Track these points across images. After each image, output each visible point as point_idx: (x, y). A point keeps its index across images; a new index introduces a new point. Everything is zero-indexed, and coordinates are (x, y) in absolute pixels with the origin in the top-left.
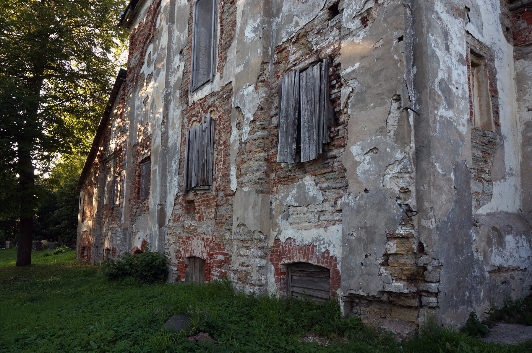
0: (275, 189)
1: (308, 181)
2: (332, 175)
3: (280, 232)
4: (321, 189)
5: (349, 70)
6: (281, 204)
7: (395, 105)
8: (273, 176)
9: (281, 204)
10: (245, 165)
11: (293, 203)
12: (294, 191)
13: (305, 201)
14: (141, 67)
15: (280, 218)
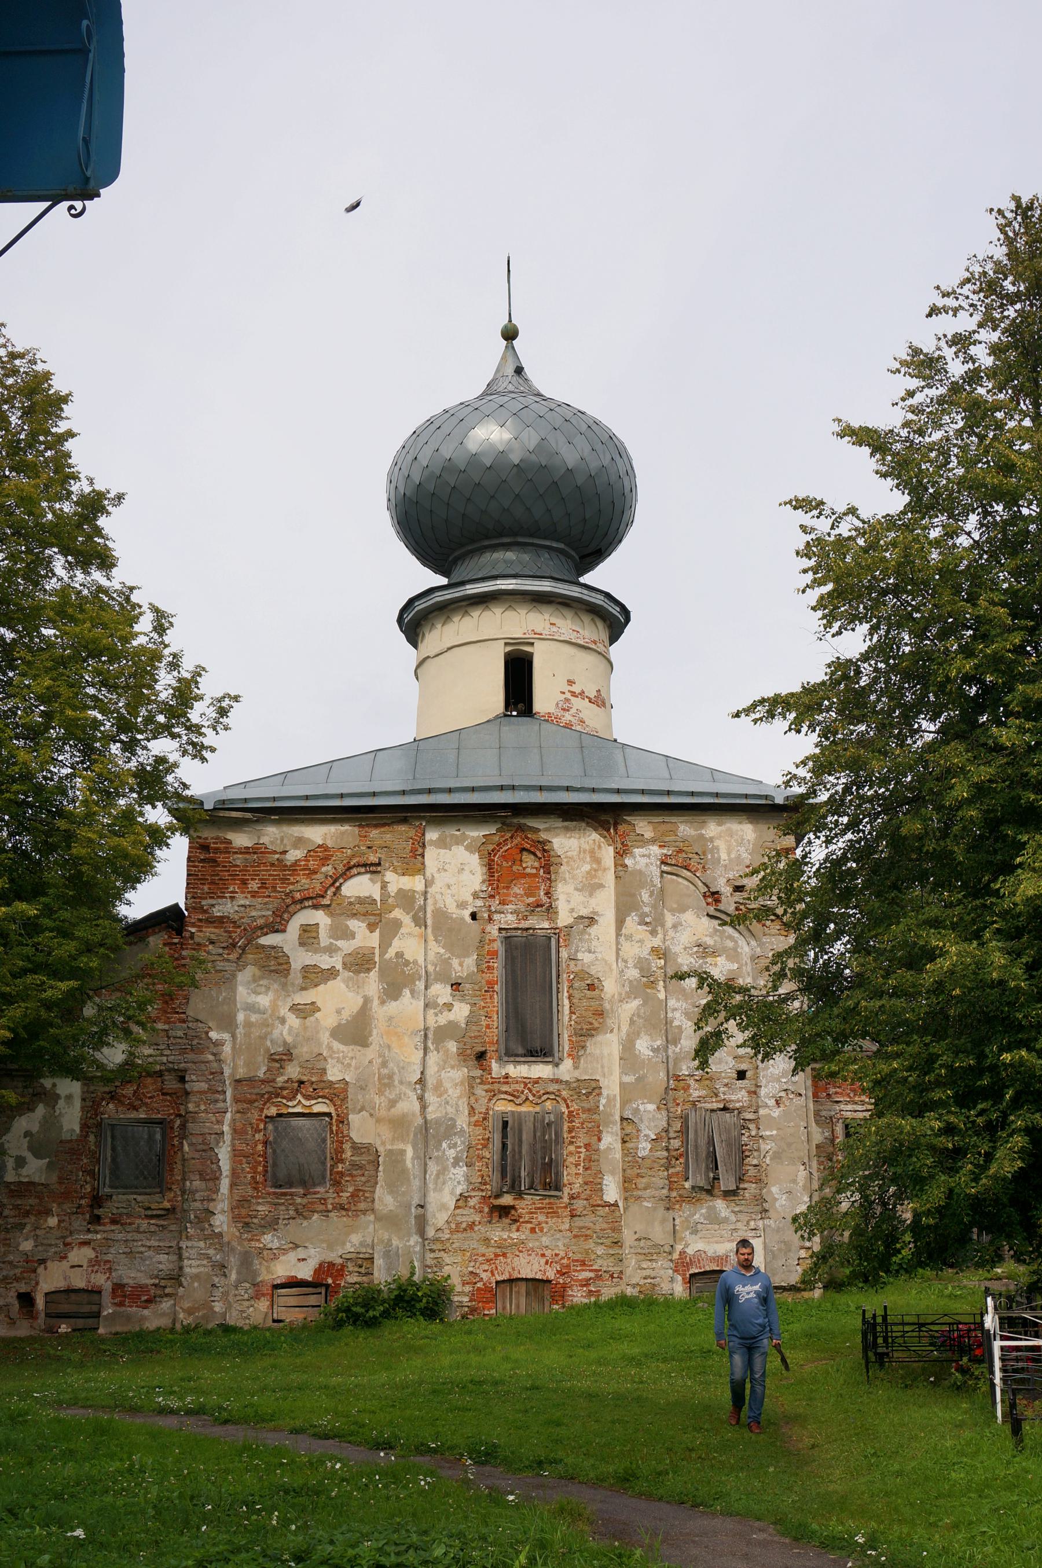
0: (677, 1206)
1: (720, 1204)
2: (743, 1202)
3: (687, 1245)
4: (733, 1212)
5: (768, 1133)
6: (687, 1220)
7: (803, 1167)
8: (674, 1194)
9: (687, 1220)
10: (644, 1180)
11: (702, 1221)
12: (704, 1211)
13: (714, 1219)
14: (266, 934)
15: (687, 1233)
